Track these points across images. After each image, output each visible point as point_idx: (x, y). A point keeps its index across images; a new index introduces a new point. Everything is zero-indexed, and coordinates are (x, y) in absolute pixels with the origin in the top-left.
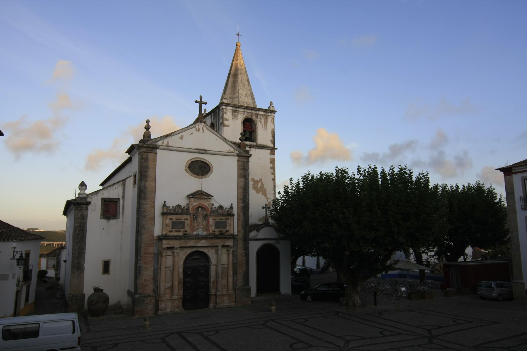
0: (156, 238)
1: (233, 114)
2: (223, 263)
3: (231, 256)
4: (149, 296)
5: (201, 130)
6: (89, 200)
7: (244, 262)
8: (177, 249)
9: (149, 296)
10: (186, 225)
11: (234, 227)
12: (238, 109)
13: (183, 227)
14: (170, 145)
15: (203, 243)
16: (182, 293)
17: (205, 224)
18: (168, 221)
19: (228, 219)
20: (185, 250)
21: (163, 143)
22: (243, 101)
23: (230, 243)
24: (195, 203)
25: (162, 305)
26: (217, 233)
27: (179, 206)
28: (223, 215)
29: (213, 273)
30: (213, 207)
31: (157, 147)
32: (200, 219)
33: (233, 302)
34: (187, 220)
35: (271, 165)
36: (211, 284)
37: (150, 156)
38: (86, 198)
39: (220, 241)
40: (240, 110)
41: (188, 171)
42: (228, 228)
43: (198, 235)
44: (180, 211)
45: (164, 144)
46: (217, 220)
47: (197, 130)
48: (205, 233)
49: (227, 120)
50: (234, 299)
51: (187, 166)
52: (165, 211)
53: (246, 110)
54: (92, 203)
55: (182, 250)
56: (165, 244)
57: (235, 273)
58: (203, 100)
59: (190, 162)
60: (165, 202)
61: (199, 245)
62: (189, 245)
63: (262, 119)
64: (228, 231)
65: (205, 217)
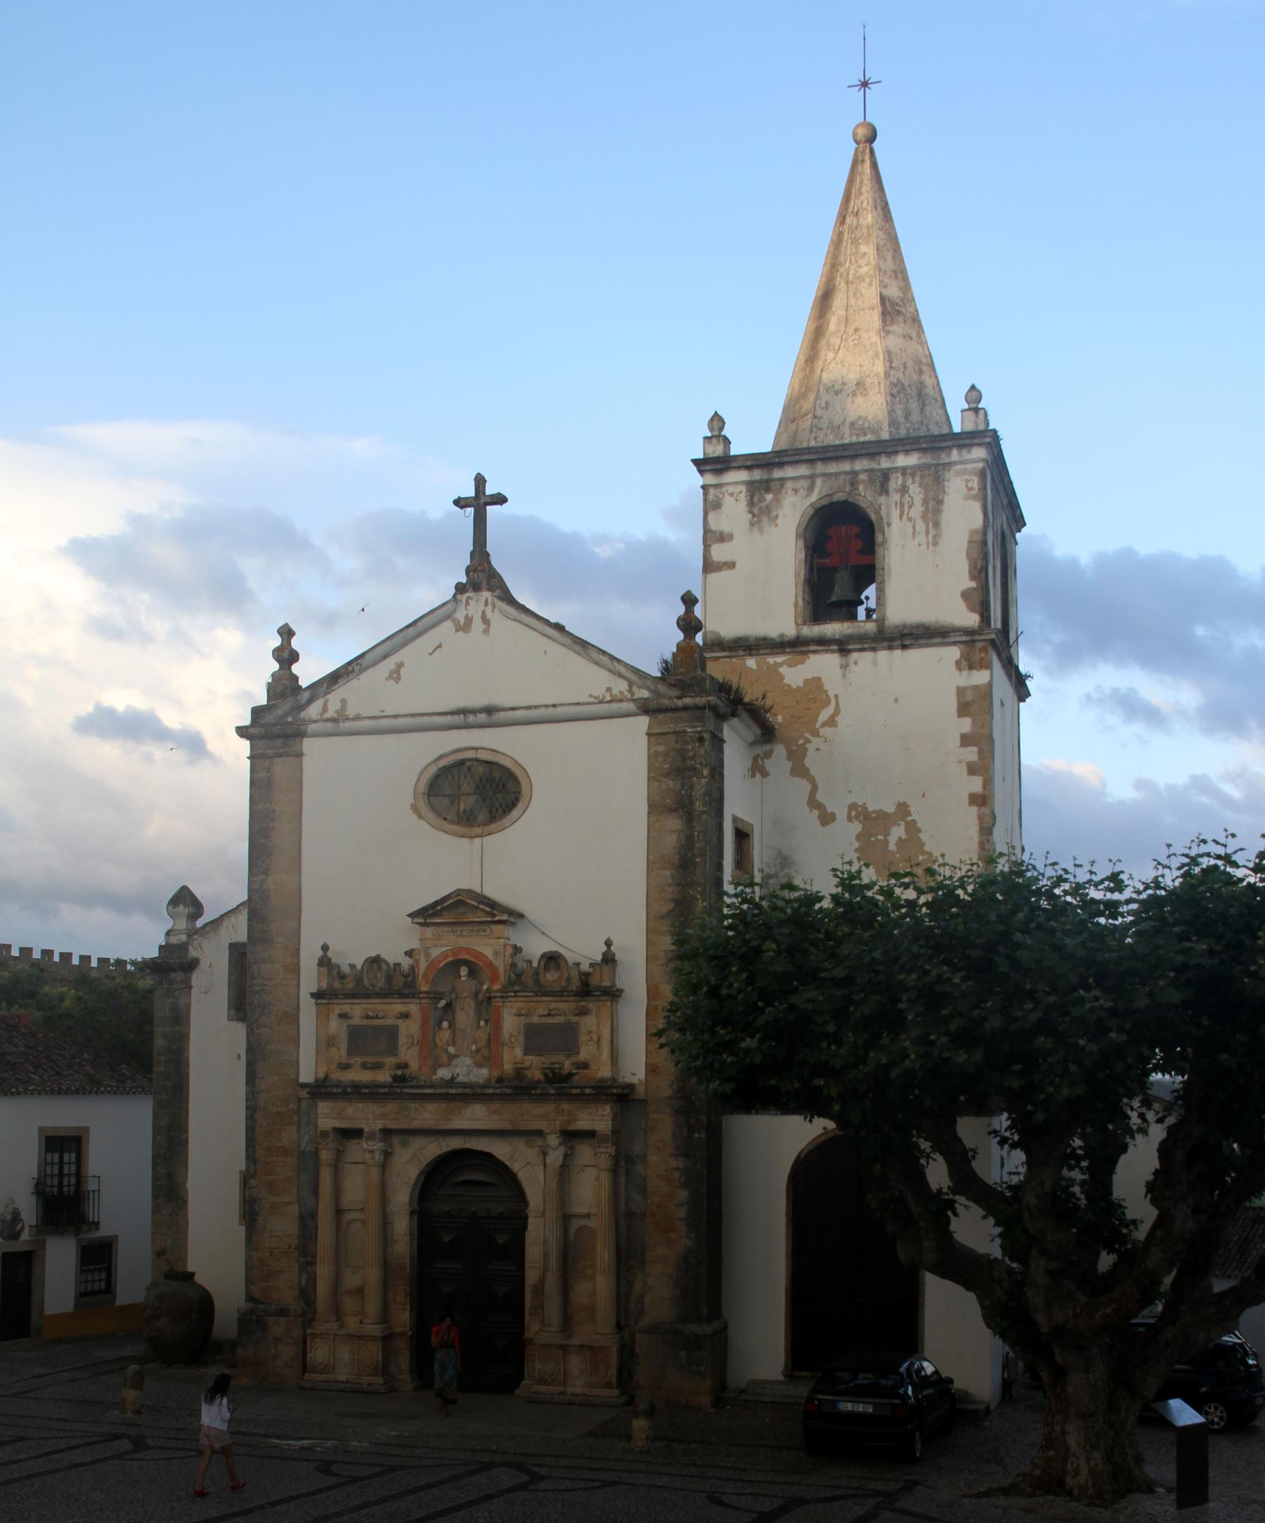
0: (304, 1094)
1: (751, 504)
2: (583, 1210)
3: (605, 1178)
4: (283, 1312)
5: (478, 624)
6: (193, 953)
7: (682, 1212)
8: (372, 1136)
9: (283, 1312)
10: (402, 1040)
11: (629, 1043)
12: (777, 474)
13: (393, 1049)
14: (351, 712)
15: (476, 1116)
16: (403, 1318)
17: (482, 1035)
18: (335, 1026)
19: (583, 1012)
20: (417, 1143)
21: (325, 709)
22: (837, 420)
23: (599, 1119)
24: (443, 945)
25: (319, 1354)
26: (537, 1075)
27: (375, 961)
28: (561, 994)
29: (533, 1252)
31: (301, 735)
32: (465, 1015)
33: (608, 1385)
34: (407, 1021)
35: (966, 725)
36: (528, 1296)
37: (281, 767)
38: (183, 947)
39: (549, 1108)
40: (789, 472)
41: (425, 809)
42: (584, 1053)
43: (452, 1082)
44: (381, 983)
45: (331, 713)
46: (535, 1019)
47: (459, 628)
48: (484, 1073)
49: (723, 538)
50: (613, 1371)
51: (423, 787)
52: (324, 985)
53: (820, 468)
54: (204, 964)
55: (405, 1145)
56: (327, 1116)
57: (628, 1257)
58: (490, 490)
59: (433, 770)
60: (325, 948)
61: (457, 1124)
62: (416, 1124)
63: (915, 491)
64: (585, 1066)
65: (486, 1005)
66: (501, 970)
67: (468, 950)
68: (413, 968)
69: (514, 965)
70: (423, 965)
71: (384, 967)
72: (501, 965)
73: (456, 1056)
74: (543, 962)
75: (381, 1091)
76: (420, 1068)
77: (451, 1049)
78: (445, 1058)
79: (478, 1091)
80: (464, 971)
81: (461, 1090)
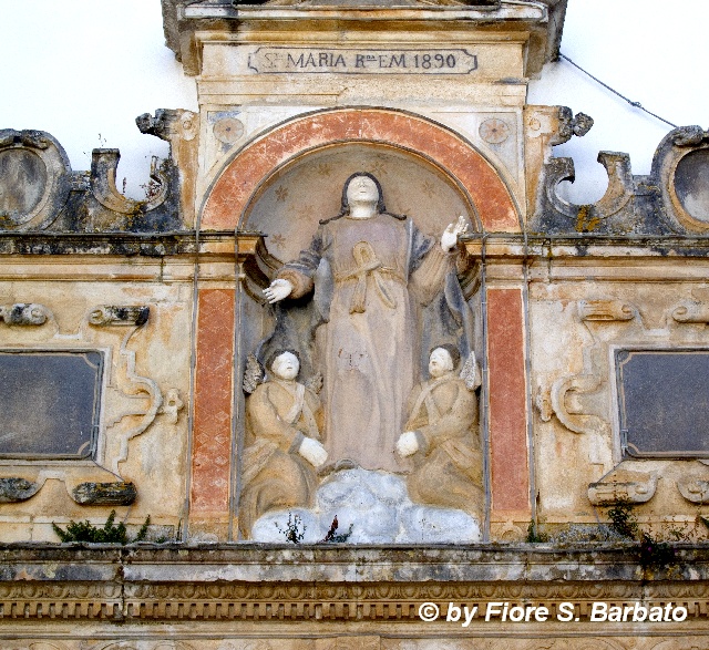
10: (113, 405)
30: (582, 148)
46: (661, 337)
66: (517, 180)
67: (385, 115)
68: (166, 173)
69: (563, 170)
70: (208, 161)
71: (49, 160)
72: (516, 165)
73: (328, 470)
74: (671, 161)
75: (26, 572)
76: (187, 509)
77: (313, 450)
78: (289, 477)
79: (456, 570)
80: (362, 192)
81: (383, 570)
